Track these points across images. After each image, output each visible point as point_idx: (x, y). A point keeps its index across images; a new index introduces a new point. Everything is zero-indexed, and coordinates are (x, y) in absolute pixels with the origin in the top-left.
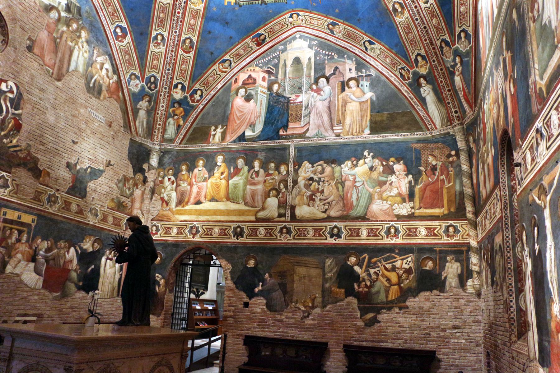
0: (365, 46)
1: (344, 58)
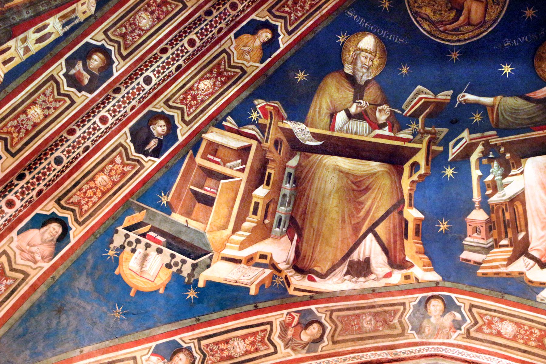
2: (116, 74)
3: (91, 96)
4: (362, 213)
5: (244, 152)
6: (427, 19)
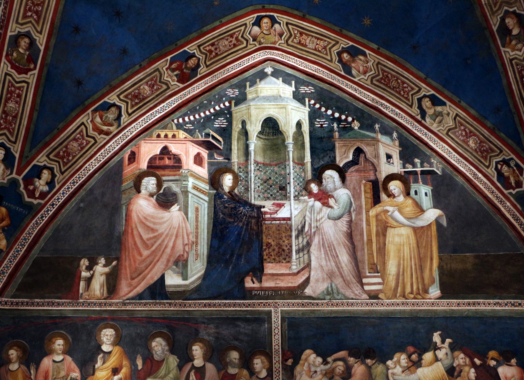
0: (420, 107)
1: (374, 131)
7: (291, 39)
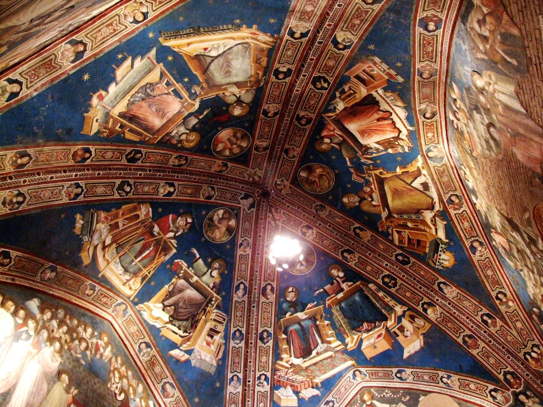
2: (388, 273)
3: (398, 279)
4: (405, 189)
5: (398, 232)
6: (329, 183)
7: (118, 20)
